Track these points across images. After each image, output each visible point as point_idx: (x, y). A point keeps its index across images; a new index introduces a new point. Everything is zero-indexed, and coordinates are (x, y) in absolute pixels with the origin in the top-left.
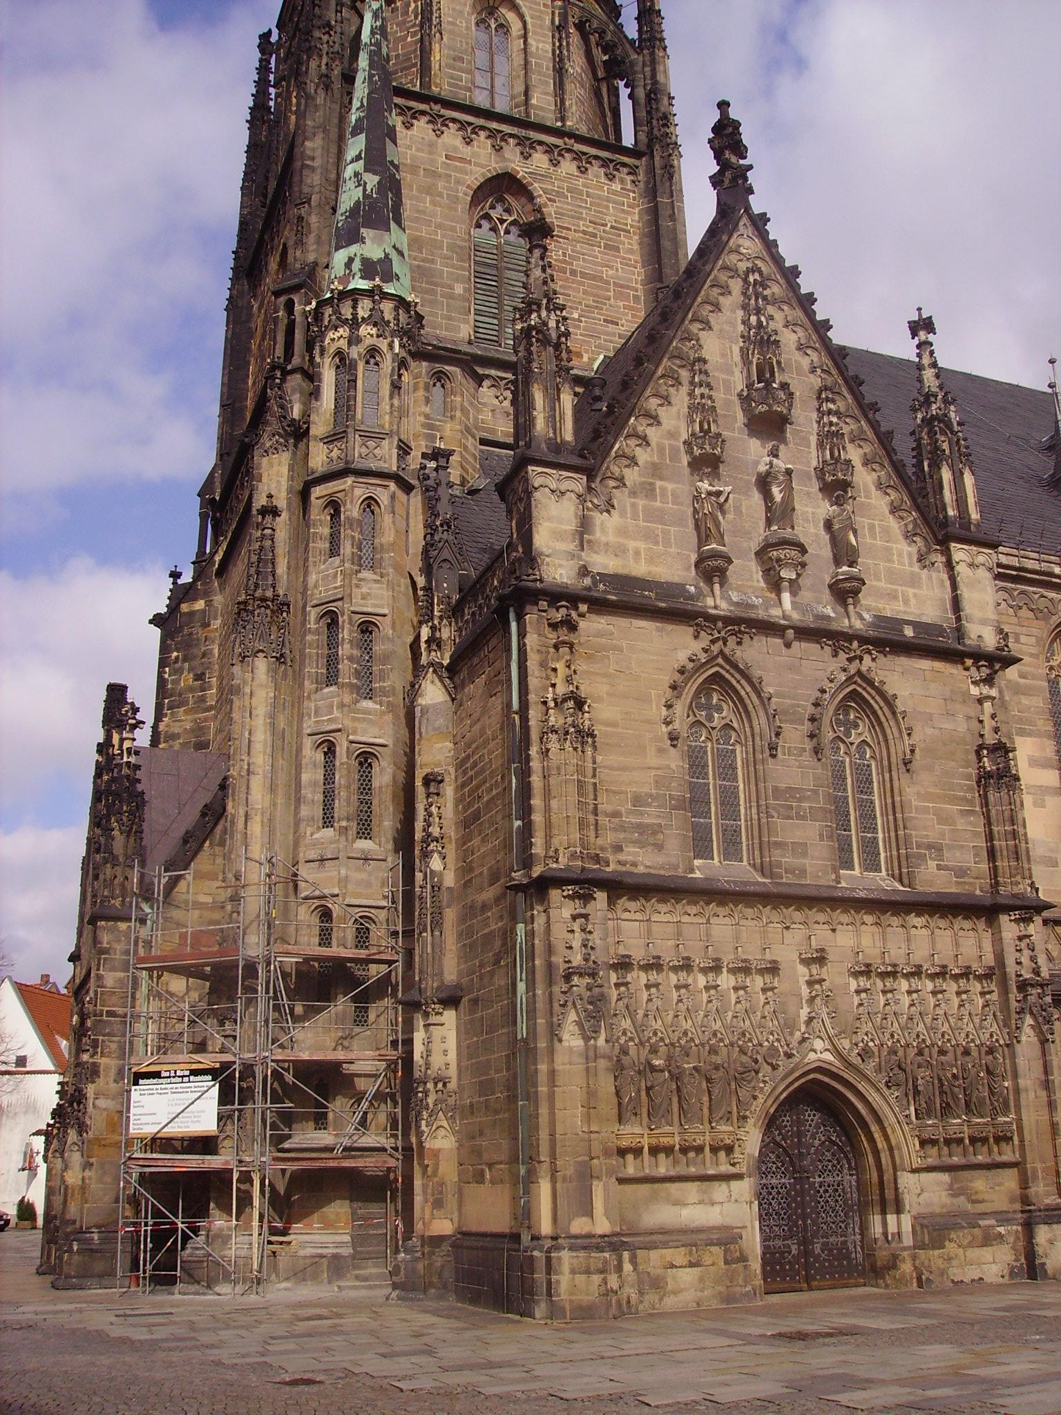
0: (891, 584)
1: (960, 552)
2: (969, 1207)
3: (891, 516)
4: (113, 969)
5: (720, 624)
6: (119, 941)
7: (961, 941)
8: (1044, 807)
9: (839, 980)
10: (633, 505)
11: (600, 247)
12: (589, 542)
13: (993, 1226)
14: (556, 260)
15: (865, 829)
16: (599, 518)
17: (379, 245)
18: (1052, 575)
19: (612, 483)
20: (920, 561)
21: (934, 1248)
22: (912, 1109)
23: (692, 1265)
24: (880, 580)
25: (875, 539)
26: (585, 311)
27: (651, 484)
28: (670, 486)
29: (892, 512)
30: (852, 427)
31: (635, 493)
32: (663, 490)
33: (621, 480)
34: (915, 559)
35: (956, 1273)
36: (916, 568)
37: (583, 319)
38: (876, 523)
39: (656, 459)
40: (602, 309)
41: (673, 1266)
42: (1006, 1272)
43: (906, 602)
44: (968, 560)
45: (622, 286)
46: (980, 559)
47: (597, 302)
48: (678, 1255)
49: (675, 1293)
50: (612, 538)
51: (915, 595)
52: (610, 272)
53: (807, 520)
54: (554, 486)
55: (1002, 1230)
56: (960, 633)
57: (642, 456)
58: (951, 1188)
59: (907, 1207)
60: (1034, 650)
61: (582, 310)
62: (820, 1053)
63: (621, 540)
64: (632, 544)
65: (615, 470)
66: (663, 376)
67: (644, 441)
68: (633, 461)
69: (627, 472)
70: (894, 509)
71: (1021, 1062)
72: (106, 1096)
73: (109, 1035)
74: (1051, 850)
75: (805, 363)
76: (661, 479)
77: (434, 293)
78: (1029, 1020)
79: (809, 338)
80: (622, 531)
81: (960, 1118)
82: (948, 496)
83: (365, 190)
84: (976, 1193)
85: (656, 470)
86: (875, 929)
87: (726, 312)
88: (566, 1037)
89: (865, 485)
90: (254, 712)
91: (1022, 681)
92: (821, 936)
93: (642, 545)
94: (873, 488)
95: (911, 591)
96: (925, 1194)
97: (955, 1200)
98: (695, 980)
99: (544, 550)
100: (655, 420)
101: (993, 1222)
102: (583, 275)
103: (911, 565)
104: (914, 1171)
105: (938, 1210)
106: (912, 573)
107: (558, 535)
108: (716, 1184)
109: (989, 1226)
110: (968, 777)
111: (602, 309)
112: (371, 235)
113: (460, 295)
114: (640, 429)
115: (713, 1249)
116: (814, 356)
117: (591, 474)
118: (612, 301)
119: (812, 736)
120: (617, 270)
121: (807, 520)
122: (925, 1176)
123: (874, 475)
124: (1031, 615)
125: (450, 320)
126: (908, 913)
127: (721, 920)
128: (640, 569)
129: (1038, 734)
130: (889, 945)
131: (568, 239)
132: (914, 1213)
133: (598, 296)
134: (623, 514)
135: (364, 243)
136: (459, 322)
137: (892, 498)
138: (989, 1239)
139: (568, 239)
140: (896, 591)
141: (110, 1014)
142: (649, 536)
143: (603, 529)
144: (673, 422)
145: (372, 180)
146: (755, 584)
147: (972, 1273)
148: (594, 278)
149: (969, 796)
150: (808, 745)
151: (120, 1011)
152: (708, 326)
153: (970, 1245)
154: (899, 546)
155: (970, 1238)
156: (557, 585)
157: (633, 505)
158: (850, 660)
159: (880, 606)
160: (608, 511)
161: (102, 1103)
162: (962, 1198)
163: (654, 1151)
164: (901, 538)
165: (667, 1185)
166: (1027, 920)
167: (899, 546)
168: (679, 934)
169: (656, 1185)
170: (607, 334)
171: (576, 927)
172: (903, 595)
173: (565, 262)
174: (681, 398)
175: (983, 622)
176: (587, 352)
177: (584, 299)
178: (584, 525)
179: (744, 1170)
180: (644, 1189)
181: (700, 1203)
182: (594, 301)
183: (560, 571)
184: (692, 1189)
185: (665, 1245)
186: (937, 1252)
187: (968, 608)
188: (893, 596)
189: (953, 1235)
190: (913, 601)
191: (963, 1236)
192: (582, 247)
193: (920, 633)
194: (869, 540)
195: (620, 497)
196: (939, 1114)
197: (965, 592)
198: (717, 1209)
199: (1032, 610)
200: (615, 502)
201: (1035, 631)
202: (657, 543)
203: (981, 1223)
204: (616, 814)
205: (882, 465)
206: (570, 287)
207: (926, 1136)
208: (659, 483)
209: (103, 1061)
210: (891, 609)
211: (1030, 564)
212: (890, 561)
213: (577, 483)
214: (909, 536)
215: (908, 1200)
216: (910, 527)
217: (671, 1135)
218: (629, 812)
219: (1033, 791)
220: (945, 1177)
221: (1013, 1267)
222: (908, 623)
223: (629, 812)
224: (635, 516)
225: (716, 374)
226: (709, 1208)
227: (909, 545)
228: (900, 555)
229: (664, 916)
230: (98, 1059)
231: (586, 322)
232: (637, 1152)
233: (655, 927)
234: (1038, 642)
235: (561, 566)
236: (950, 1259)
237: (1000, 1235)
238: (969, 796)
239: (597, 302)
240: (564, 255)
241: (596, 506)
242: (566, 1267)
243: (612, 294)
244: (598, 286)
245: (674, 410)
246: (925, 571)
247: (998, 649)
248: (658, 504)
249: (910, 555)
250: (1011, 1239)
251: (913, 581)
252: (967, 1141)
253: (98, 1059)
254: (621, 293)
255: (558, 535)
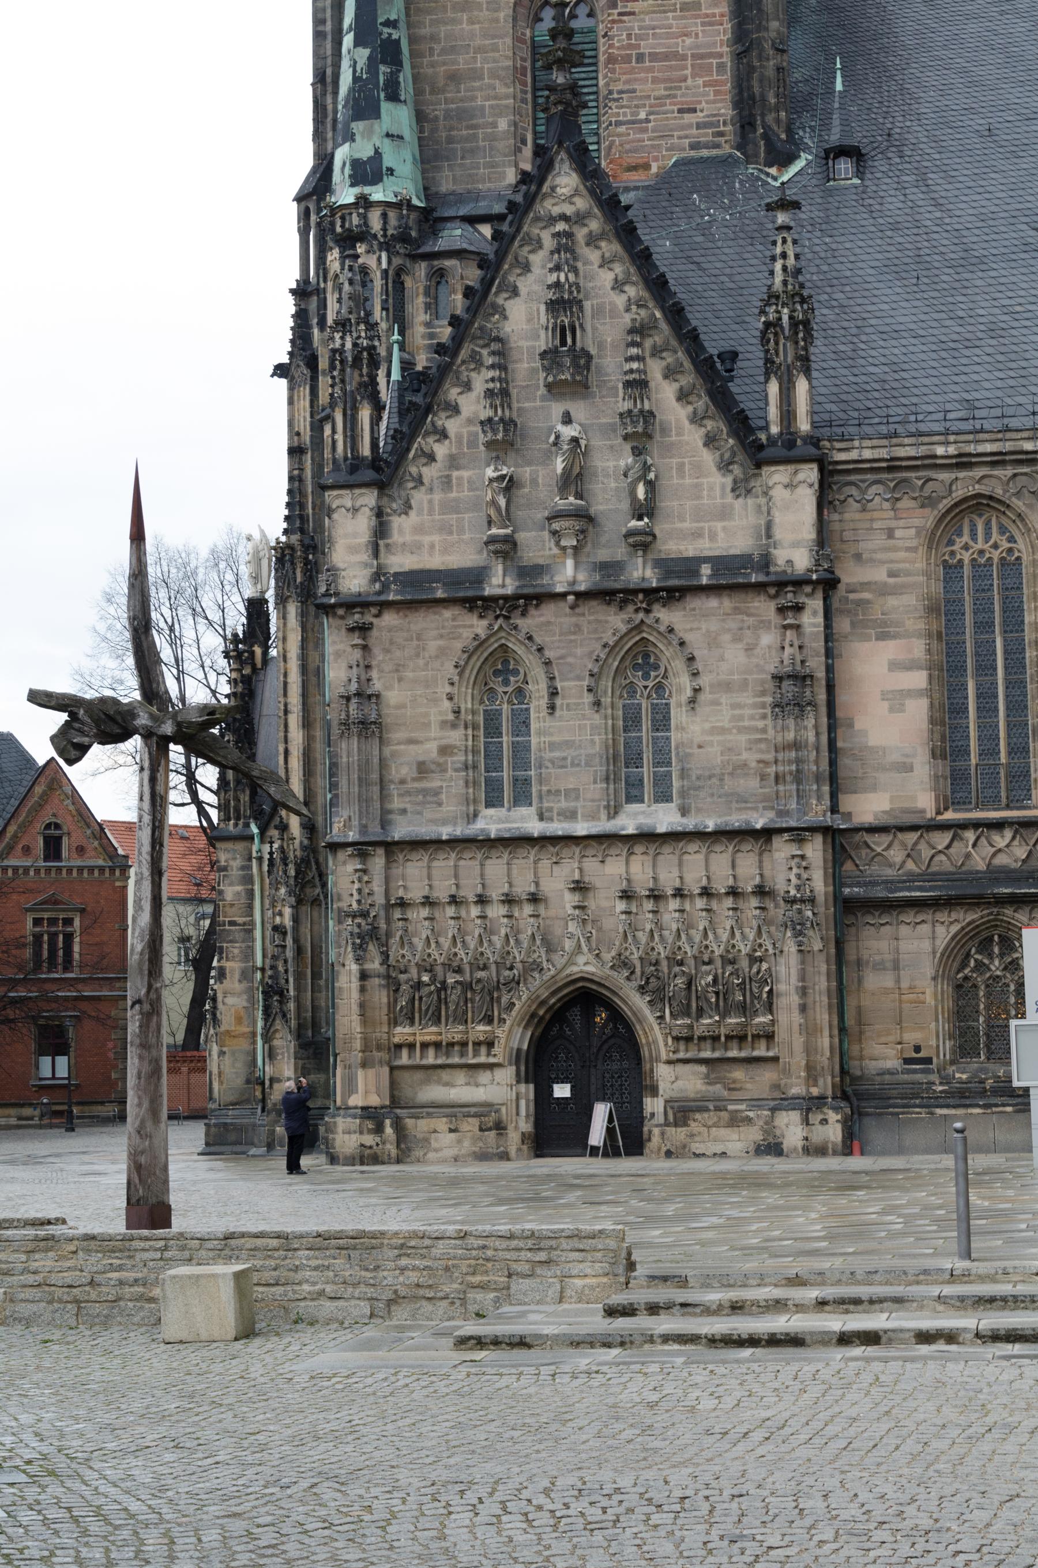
0: (698, 521)
1: (777, 476)
2: (726, 1093)
3: (705, 450)
4: (231, 884)
5: (501, 602)
6: (235, 859)
7: (739, 862)
8: (903, 711)
9: (605, 904)
10: (430, 502)
11: (675, 11)
12: (387, 546)
13: (742, 1111)
14: (618, 48)
15: (657, 764)
16: (397, 522)
17: (369, 139)
18: (935, 457)
19: (411, 485)
20: (733, 490)
21: (676, 1125)
22: (667, 1011)
23: (451, 1131)
24: (682, 519)
25: (683, 478)
26: (656, 105)
27: (448, 477)
28: (465, 474)
29: (706, 445)
30: (670, 360)
31: (431, 489)
32: (460, 479)
33: (419, 481)
34: (729, 489)
35: (697, 1147)
36: (729, 498)
37: (652, 117)
38: (686, 460)
39: (454, 451)
40: (675, 96)
41: (435, 1131)
42: (752, 1148)
43: (713, 537)
44: (786, 480)
45: (702, 56)
46: (801, 476)
47: (671, 88)
48: (442, 1124)
49: (436, 1150)
50: (408, 538)
51: (724, 528)
52: (688, 41)
53: (608, 476)
54: (349, 504)
55: (751, 1114)
56: (766, 562)
57: (441, 450)
58: (707, 1076)
59: (661, 1092)
60: (914, 543)
61: (651, 106)
62: (585, 965)
63: (417, 538)
64: (427, 539)
65: (413, 470)
66: (463, 362)
67: (443, 435)
68: (431, 458)
69: (425, 470)
70: (710, 441)
71: (782, 969)
72: (233, 994)
73: (231, 941)
74: (907, 756)
75: (620, 301)
76: (458, 469)
77: (475, 137)
78: (789, 934)
79: (628, 273)
80: (419, 529)
81: (711, 1017)
82: (773, 412)
83: (354, 71)
84: (734, 1082)
85: (453, 462)
86: (645, 857)
87: (537, 270)
88: (347, 963)
89: (677, 420)
90: (289, 655)
91: (891, 580)
92: (591, 865)
93: (436, 538)
94: (686, 423)
95: (719, 525)
96: (680, 1083)
97: (710, 1088)
98: (468, 912)
99: (341, 565)
100: (454, 410)
101: (743, 1107)
102: (654, 57)
103: (723, 496)
104: (669, 1062)
105: (692, 1096)
106: (724, 506)
107: (353, 550)
108: (481, 1072)
109: (736, 1111)
110: (763, 706)
111: (675, 96)
112: (361, 128)
113: (504, 132)
114: (440, 423)
115: (470, 1120)
116: (631, 291)
117: (382, 486)
118: (689, 81)
119: (590, 690)
120: (697, 35)
121: (608, 476)
122: (681, 1068)
123: (690, 409)
124: (912, 504)
125: (493, 167)
126: (681, 840)
127: (494, 861)
128: (435, 562)
129: (907, 635)
130: (659, 870)
131: (633, 13)
132: (667, 1097)
133: (670, 80)
134: (420, 513)
135: (354, 140)
136: (504, 166)
137: (709, 428)
138: (735, 1121)
139: (633, 13)
140: (702, 528)
141: (232, 923)
142: (445, 529)
143: (401, 531)
144: (473, 408)
145: (363, 54)
146: (547, 553)
147: (719, 1148)
148: (666, 57)
149: (760, 724)
150: (588, 699)
151: (240, 920)
152: (515, 292)
153: (715, 1125)
154: (711, 480)
155: (715, 1119)
156: (352, 595)
157: (430, 502)
158: (637, 611)
159: (682, 548)
160: (406, 514)
161: (230, 1000)
162: (719, 1086)
163: (425, 1046)
164: (714, 469)
165: (439, 1071)
166: (800, 841)
167: (711, 480)
168: (456, 876)
169: (430, 1072)
170: (682, 128)
171: (355, 878)
172: (710, 531)
173: (630, 46)
174: (480, 381)
175: (796, 545)
176: (656, 159)
177: (653, 90)
178: (381, 530)
179: (501, 1060)
180: (419, 1075)
181: (468, 1084)
182: (666, 89)
183: (356, 582)
184: (460, 1077)
185: (429, 1115)
186: (679, 1129)
187: (778, 534)
188: (697, 534)
189: (698, 1116)
190: (721, 535)
191: (710, 1117)
192: (652, 20)
193: (718, 570)
194: (675, 481)
195: (419, 497)
196: (694, 1015)
197: (778, 517)
198: (481, 1090)
199: (915, 499)
200: (413, 502)
201: (917, 522)
202: (451, 533)
203: (730, 1107)
204: (403, 782)
205: (699, 396)
206: (636, 80)
207: (674, 1034)
208: (455, 474)
209: (228, 965)
210: (690, 549)
211: (901, 452)
212: (699, 497)
213: (369, 498)
214: (724, 466)
215: (662, 1086)
216: (727, 455)
217: (454, 1032)
218: (414, 780)
219: (890, 696)
220: (703, 1069)
221: (759, 1146)
222: (706, 560)
223: (414, 780)
224: (431, 512)
225: (520, 344)
226: (474, 1089)
227: (724, 475)
228: (711, 489)
229: (444, 864)
230: (224, 963)
231: (655, 120)
232: (411, 1046)
233: (434, 872)
234: (918, 534)
235: (355, 577)
236: (692, 1135)
237: (749, 1120)
238: (760, 724)
239: (671, 88)
240: (629, 36)
241: (395, 511)
242: (340, 1129)
243: (688, 72)
244: (671, 67)
245: (472, 395)
246: (740, 500)
247: (810, 571)
248: (454, 495)
249: (723, 487)
250: (761, 1123)
251: (724, 514)
252: (723, 1039)
253: (224, 963)
254: (701, 66)
255: (353, 550)
